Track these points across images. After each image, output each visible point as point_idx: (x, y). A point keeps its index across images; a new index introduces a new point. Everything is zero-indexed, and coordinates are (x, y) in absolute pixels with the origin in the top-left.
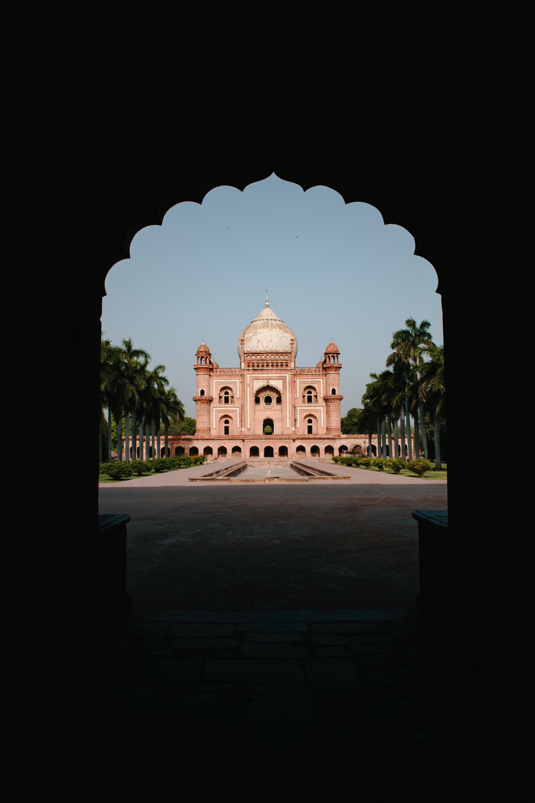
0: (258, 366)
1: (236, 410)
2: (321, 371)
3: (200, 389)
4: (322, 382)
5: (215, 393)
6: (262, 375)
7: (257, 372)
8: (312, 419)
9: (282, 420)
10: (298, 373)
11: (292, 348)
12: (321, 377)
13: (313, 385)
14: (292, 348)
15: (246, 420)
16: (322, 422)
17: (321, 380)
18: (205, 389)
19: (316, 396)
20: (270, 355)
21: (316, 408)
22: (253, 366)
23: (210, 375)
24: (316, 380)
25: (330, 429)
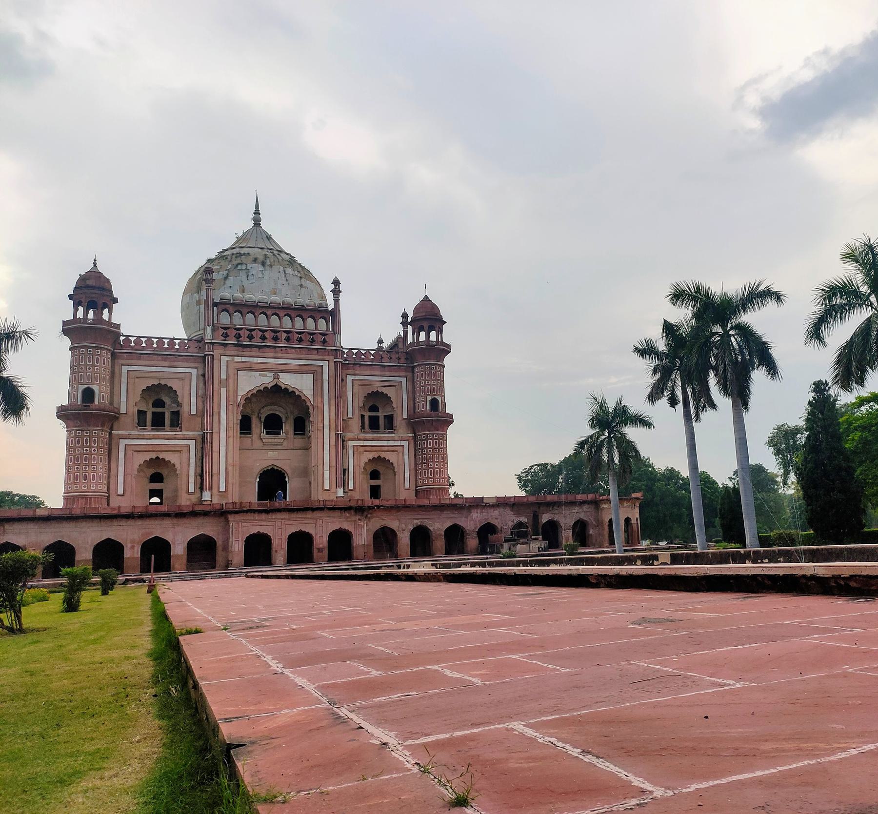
0: (251, 337)
1: (189, 446)
2: (402, 360)
3: (82, 387)
4: (404, 385)
5: (127, 401)
6: (260, 360)
7: (247, 352)
8: (381, 469)
9: (305, 472)
10: (350, 362)
11: (337, 301)
12: (403, 374)
13: (385, 391)
14: (337, 301)
15: (215, 471)
16: (407, 475)
17: (404, 380)
18: (96, 388)
19: (390, 419)
20: (281, 314)
21: (391, 443)
22: (238, 337)
23: (113, 354)
24: (391, 379)
25: (429, 491)
